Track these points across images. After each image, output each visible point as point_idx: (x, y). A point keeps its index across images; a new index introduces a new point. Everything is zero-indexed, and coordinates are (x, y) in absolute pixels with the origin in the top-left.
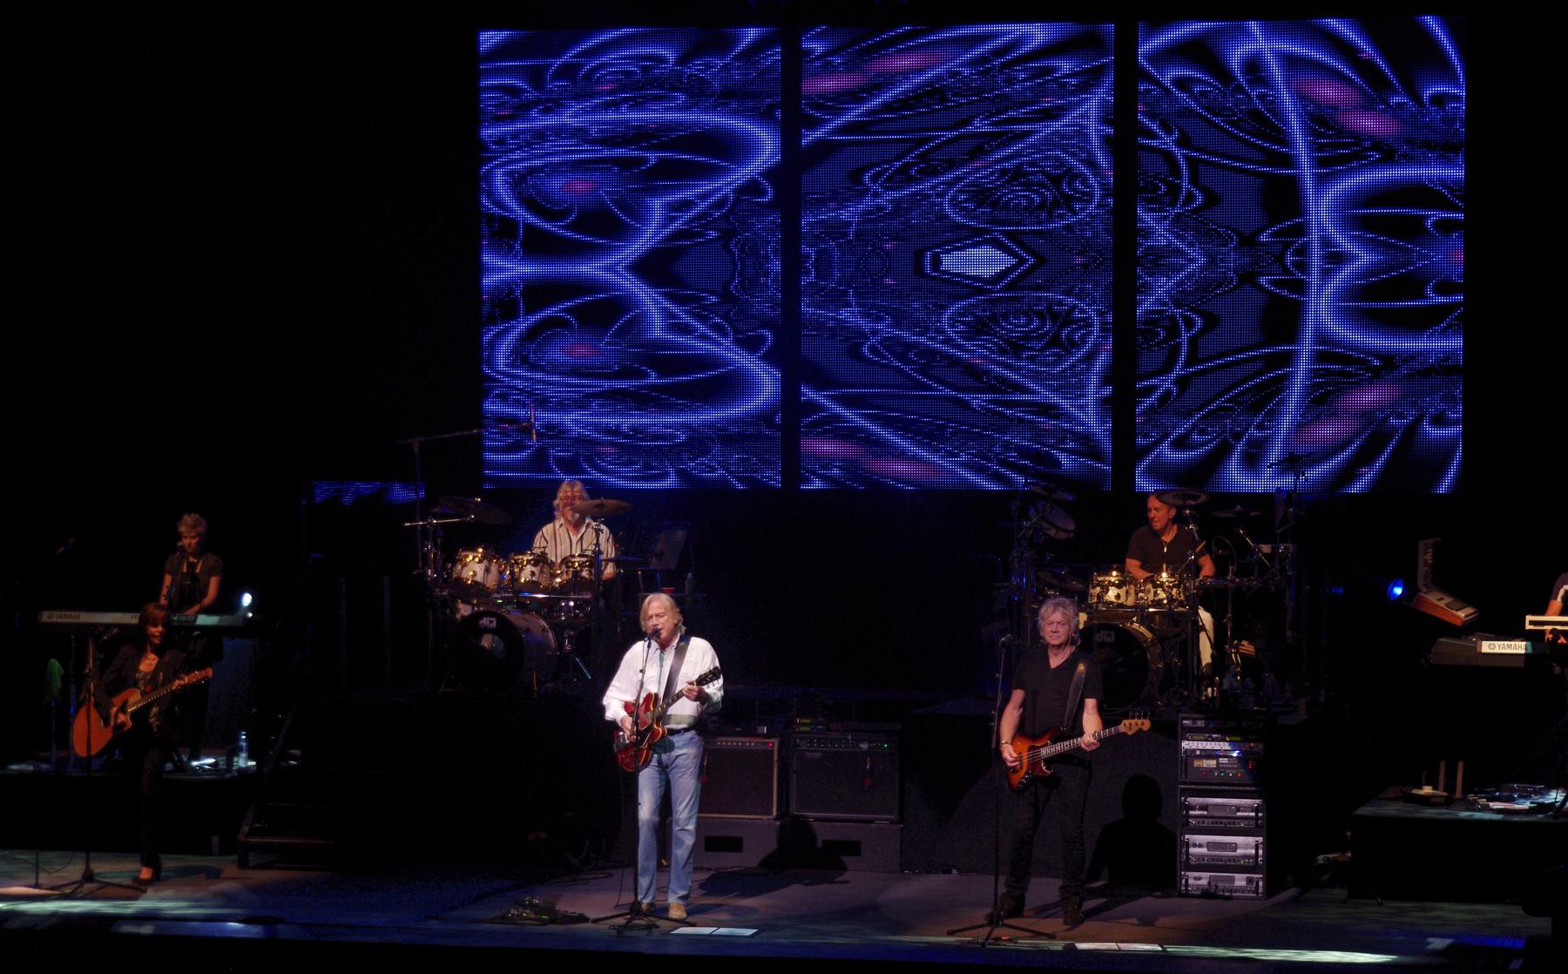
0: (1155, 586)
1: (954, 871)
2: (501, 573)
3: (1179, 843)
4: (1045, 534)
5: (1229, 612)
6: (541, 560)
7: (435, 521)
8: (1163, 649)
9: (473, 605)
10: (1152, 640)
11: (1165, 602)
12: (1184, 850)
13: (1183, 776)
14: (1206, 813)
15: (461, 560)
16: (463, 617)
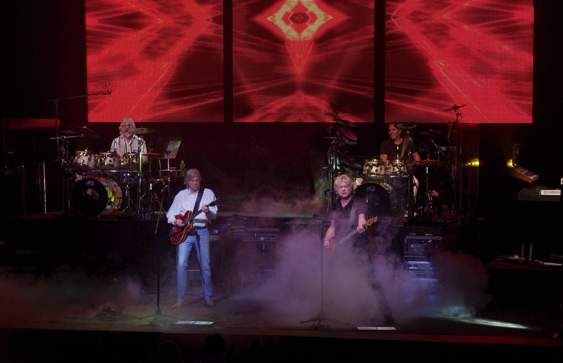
0: (394, 166)
2: (96, 161)
4: (344, 143)
6: (114, 155)
7: (65, 137)
9: (83, 176)
11: (398, 173)
13: (406, 252)
14: (416, 268)
15: (78, 155)
16: (78, 181)
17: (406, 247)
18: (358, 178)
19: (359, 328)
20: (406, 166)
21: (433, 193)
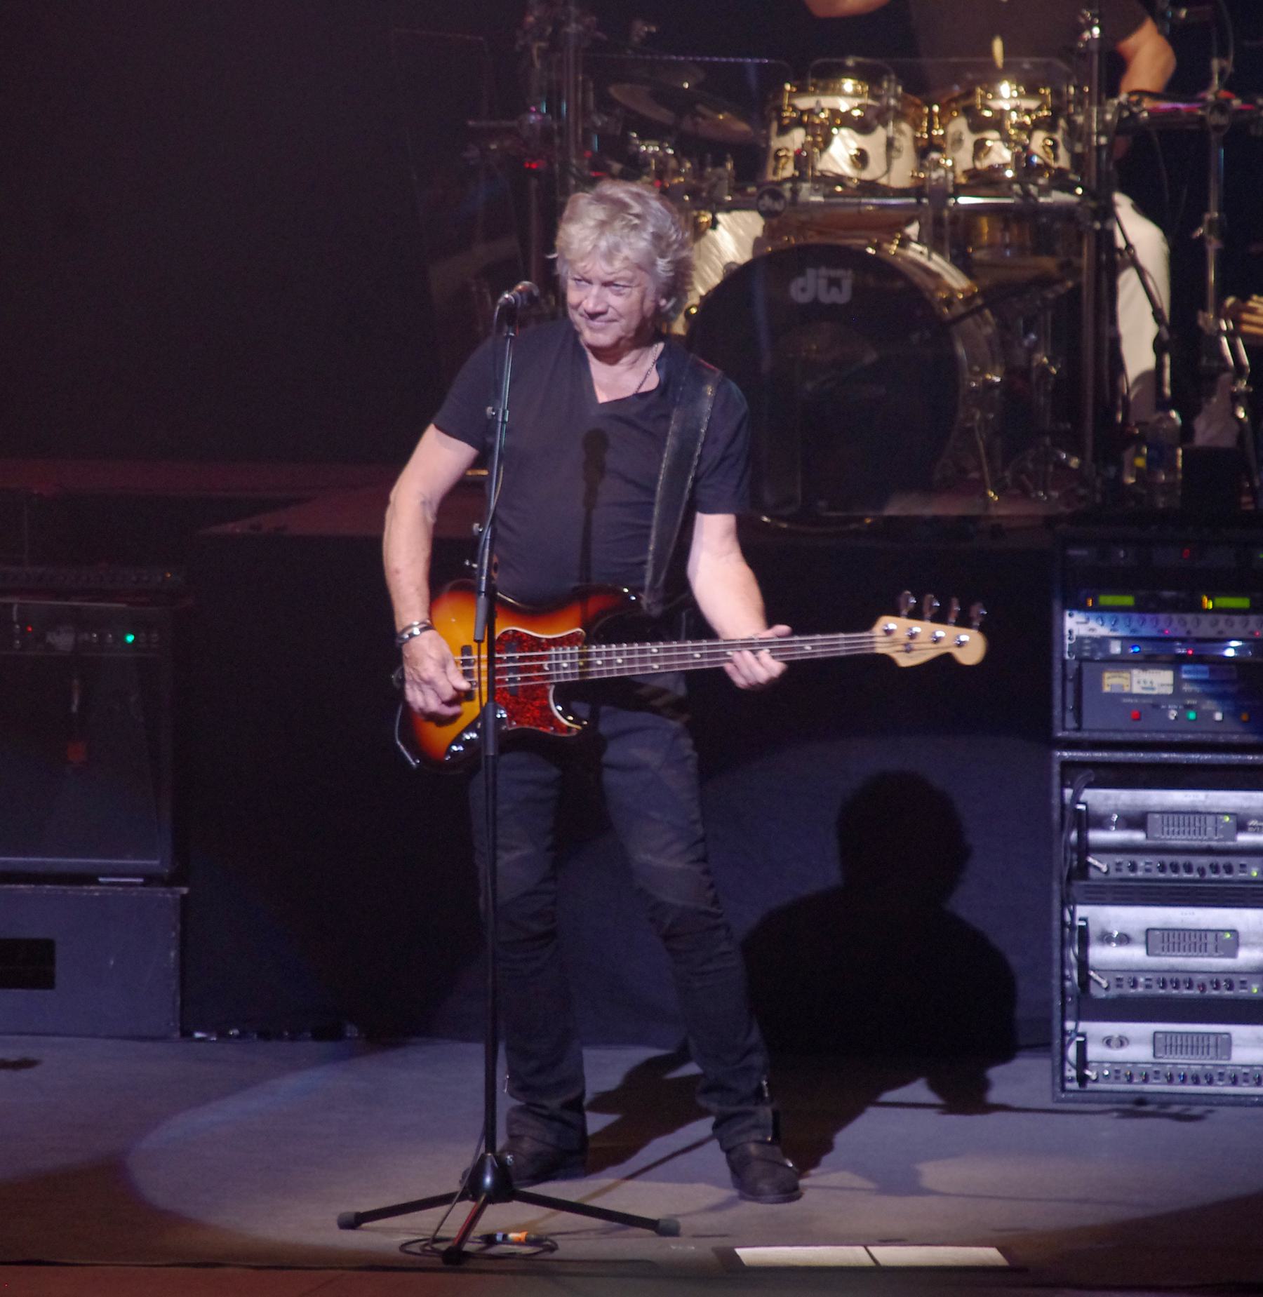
0: (978, 125)
1: (351, 1030)
3: (1056, 934)
5: (1213, 201)
8: (1004, 326)
10: (968, 300)
11: (1009, 174)
13: (1071, 723)
14: (1138, 836)
17: (1070, 686)
18: (729, 209)
19: (748, 1254)
20: (1062, 123)
21: (1254, 319)
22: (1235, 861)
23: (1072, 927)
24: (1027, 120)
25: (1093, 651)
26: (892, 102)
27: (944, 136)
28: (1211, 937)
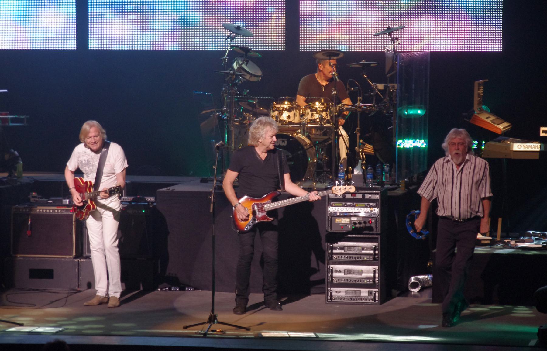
0: (312, 110)
10: (310, 145)
11: (318, 120)
12: (330, 275)
13: (329, 229)
14: (343, 251)
17: (329, 221)
22: (362, 256)
23: (330, 269)
24: (322, 110)
25: (334, 215)
26: (295, 106)
27: (305, 113)
28: (357, 271)
